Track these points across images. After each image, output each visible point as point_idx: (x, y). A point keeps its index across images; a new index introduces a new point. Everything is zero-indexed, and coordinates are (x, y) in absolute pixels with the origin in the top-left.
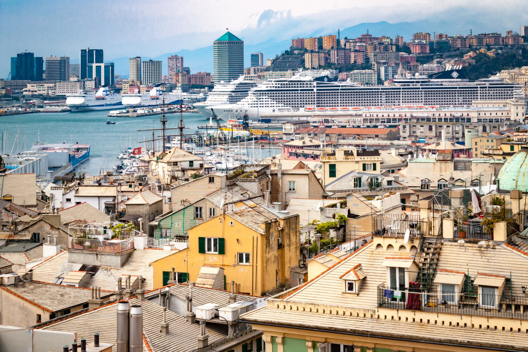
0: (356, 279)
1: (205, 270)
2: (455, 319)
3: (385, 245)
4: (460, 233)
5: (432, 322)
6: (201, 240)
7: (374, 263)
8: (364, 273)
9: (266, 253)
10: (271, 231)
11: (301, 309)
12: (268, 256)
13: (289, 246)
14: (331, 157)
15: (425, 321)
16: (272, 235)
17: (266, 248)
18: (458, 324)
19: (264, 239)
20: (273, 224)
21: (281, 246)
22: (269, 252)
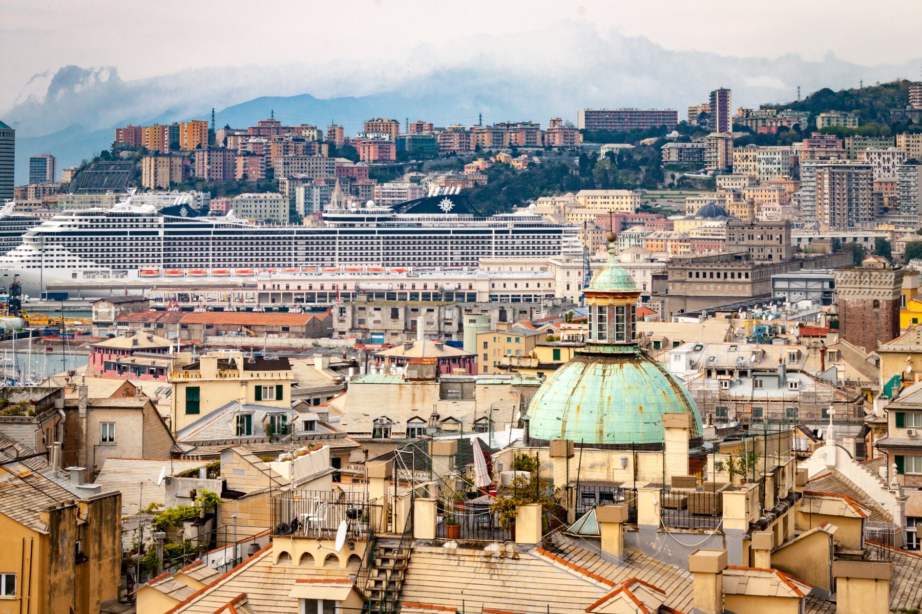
3: (296, 555)
4: (448, 528)
7: (273, 592)
9: (50, 573)
12: (54, 579)
13: (99, 557)
14: (191, 372)
17: (51, 562)
19: (47, 543)
20: (67, 512)
21: (81, 559)
22: (56, 572)
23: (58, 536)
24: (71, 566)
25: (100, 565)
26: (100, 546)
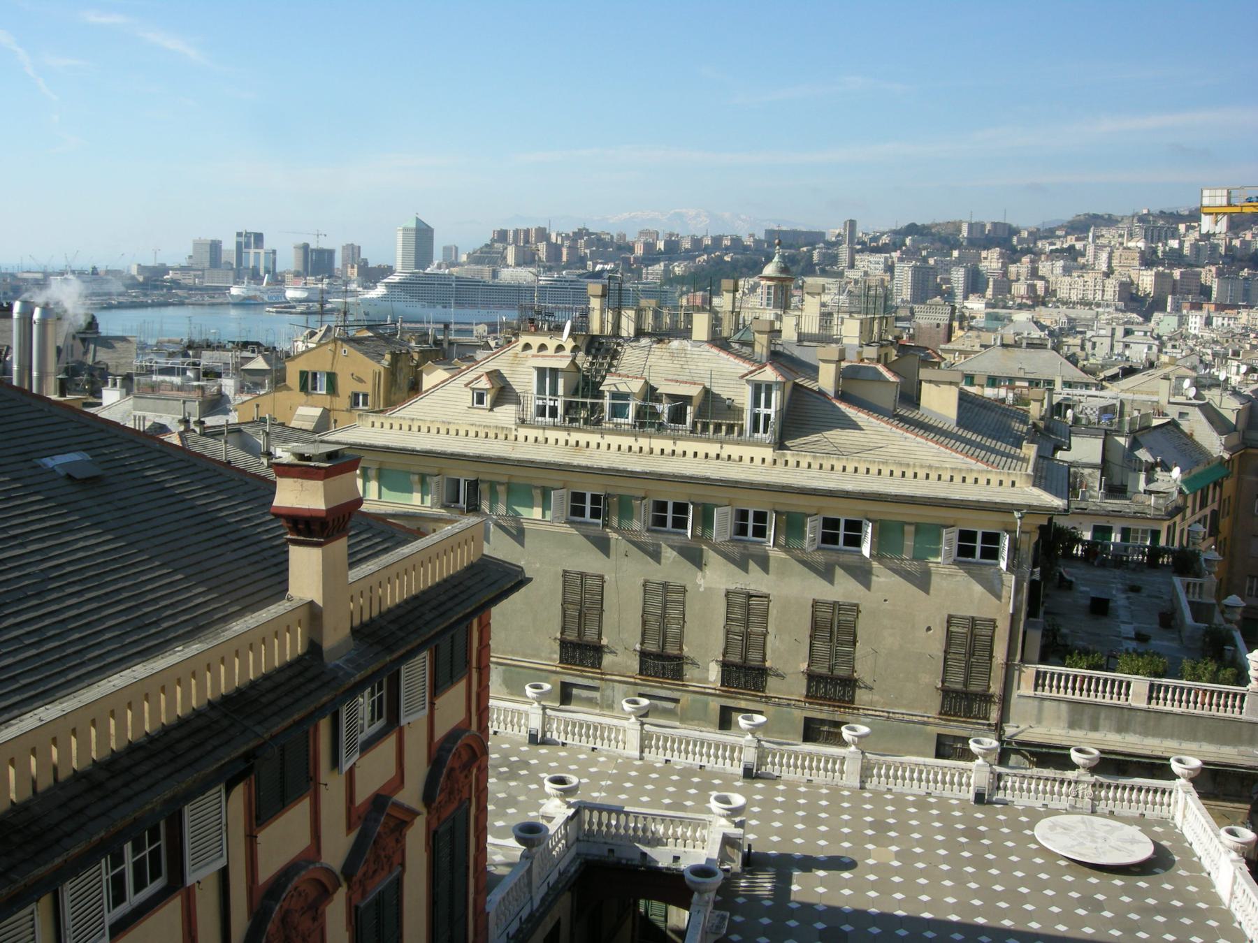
0: (488, 386)
1: (302, 411)
2: (626, 441)
5: (593, 445)
6: (303, 375)
10: (399, 365)
15: (583, 443)
18: (630, 448)
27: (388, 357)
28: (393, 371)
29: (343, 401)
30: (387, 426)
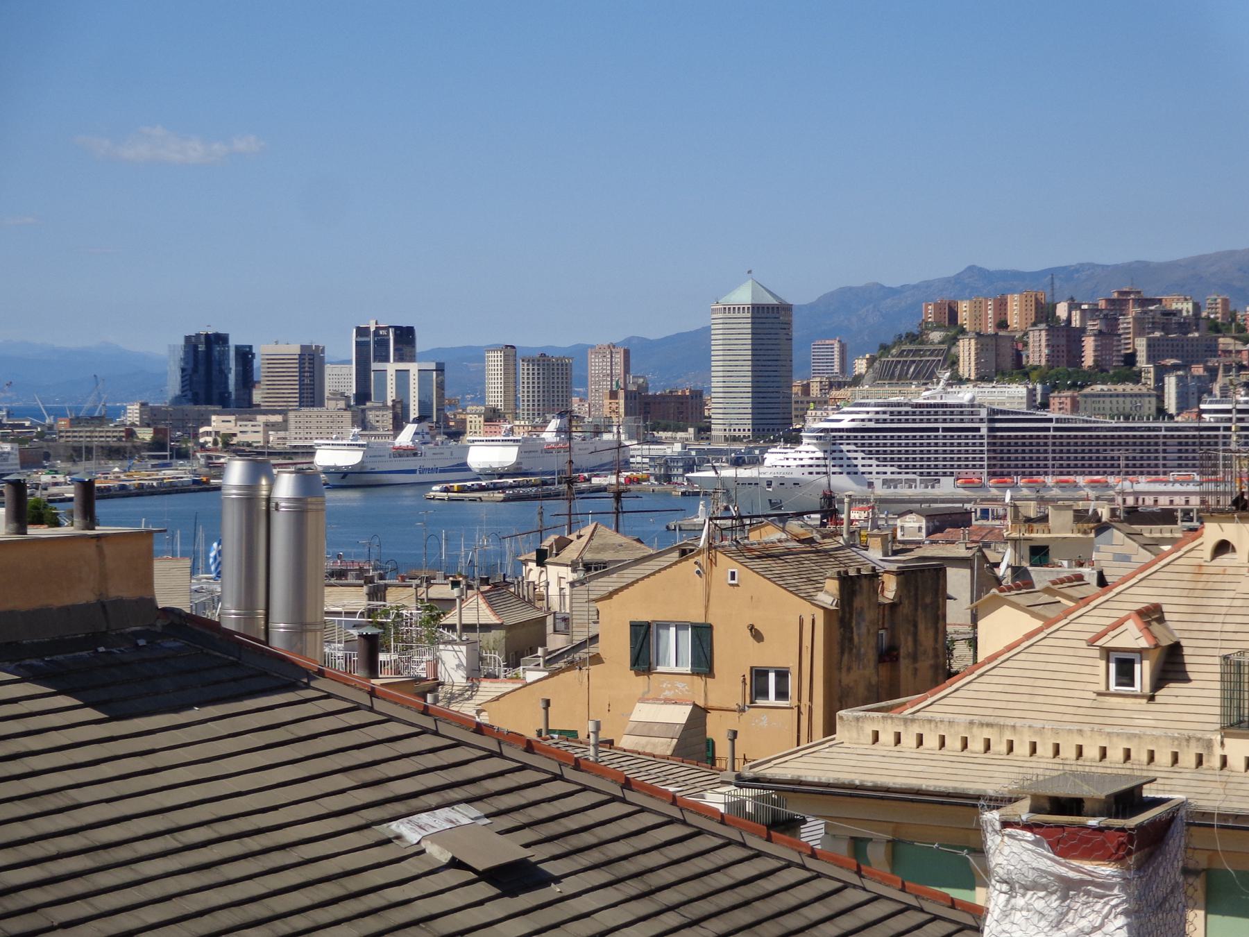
0: (1143, 643)
1: (645, 713)
7: (1205, 602)
8: (1171, 631)
9: (840, 669)
10: (857, 603)
11: (954, 743)
12: (847, 679)
13: (914, 658)
14: (1036, 526)
16: (861, 613)
17: (842, 653)
19: (836, 624)
20: (865, 582)
21: (888, 655)
22: (849, 669)
23: (851, 615)
24: (872, 664)
25: (916, 670)
26: (915, 641)
27: (832, 586)
28: (841, 622)
29: (726, 687)
30: (909, 741)
